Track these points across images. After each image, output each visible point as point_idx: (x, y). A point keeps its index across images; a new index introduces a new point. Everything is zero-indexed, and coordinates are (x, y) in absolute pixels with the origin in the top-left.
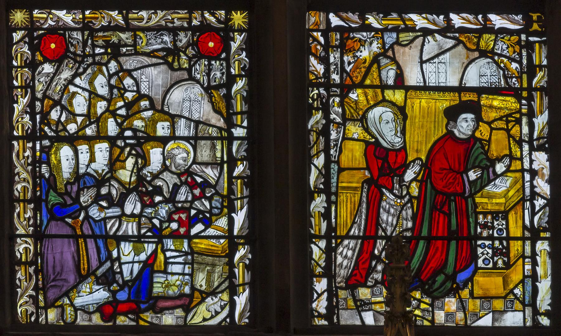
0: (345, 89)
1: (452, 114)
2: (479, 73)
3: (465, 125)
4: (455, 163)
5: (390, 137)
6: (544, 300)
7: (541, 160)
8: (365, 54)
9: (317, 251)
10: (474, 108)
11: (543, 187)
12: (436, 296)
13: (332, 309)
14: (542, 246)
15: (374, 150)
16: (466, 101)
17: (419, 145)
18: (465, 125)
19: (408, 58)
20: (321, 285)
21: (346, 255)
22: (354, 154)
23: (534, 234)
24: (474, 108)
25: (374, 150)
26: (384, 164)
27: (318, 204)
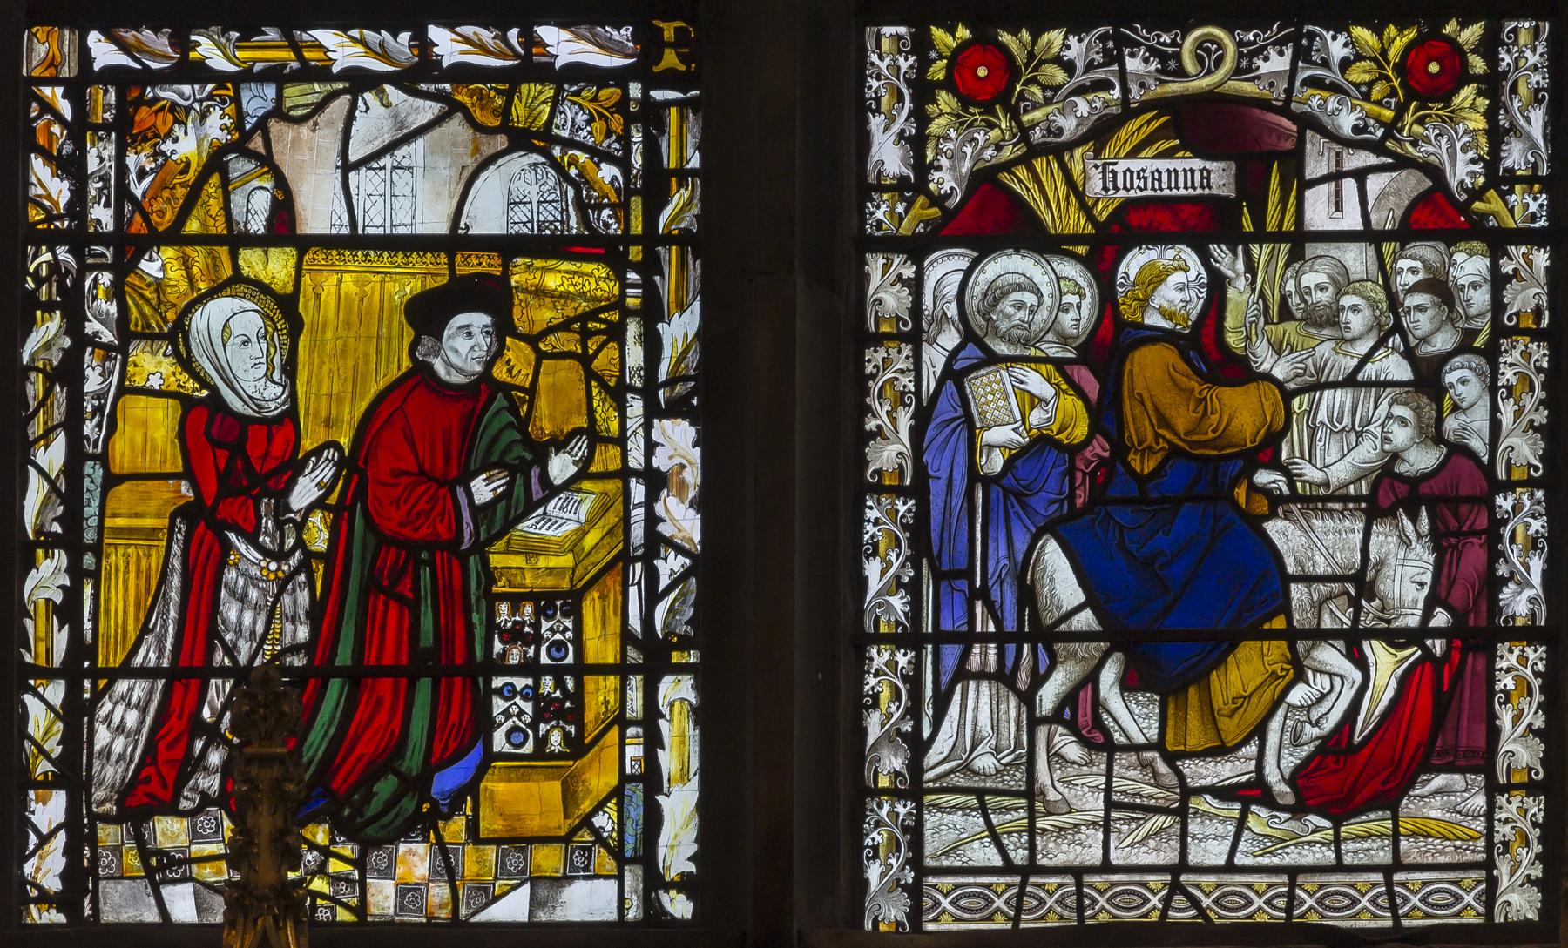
0: (127, 248)
1: (428, 315)
2: (508, 197)
3: (463, 346)
4: (434, 453)
5: (252, 382)
6: (678, 847)
7: (678, 442)
8: (186, 146)
9: (40, 716)
10: (492, 296)
11: (683, 520)
12: (373, 838)
13: (80, 878)
14: (677, 691)
15: (207, 421)
16: (469, 275)
17: (334, 407)
18: (463, 346)
19: (309, 158)
20: (49, 811)
21: (122, 724)
22: (149, 433)
23: (650, 656)
24: (492, 296)
25: (207, 421)
26: (233, 459)
27: (46, 578)
